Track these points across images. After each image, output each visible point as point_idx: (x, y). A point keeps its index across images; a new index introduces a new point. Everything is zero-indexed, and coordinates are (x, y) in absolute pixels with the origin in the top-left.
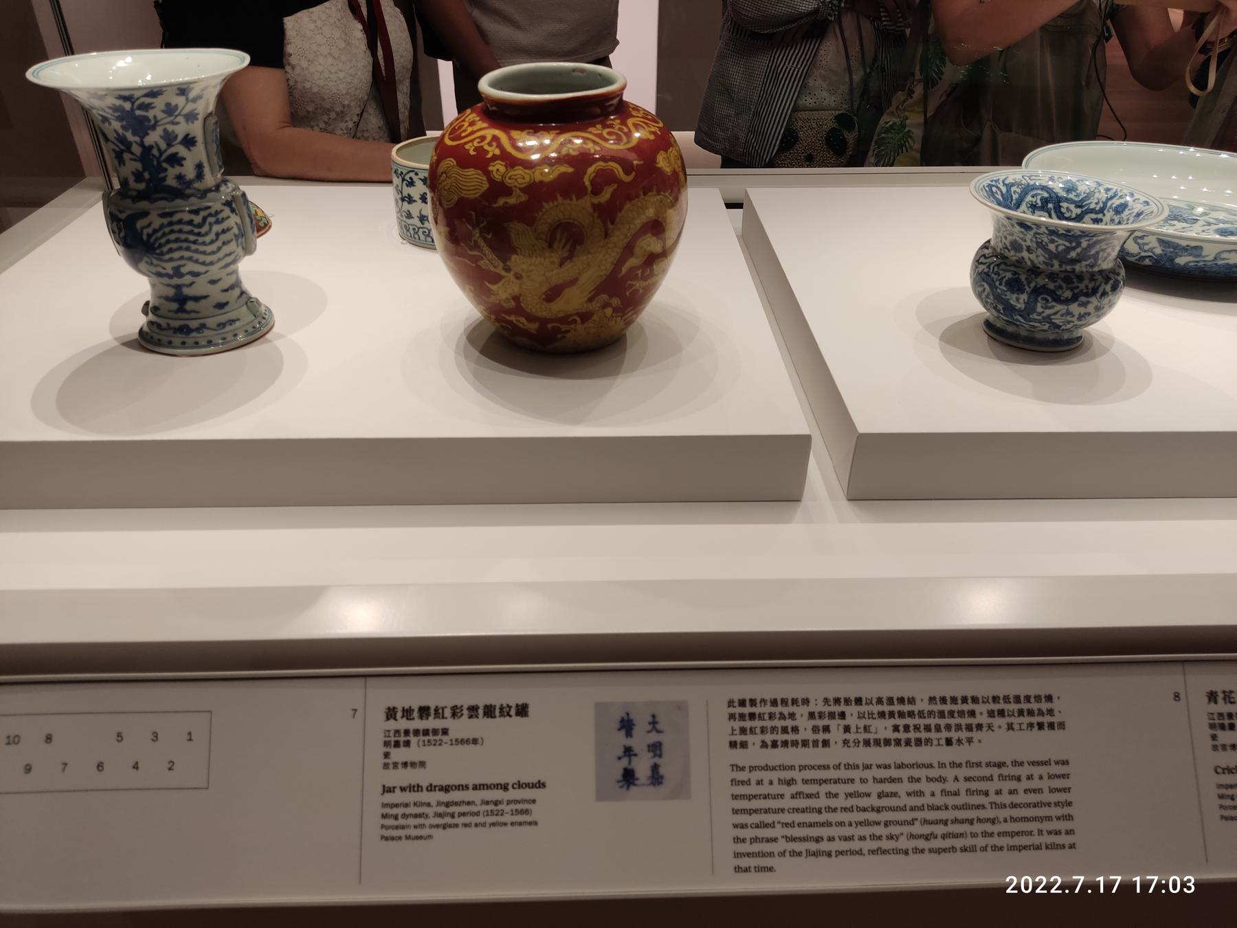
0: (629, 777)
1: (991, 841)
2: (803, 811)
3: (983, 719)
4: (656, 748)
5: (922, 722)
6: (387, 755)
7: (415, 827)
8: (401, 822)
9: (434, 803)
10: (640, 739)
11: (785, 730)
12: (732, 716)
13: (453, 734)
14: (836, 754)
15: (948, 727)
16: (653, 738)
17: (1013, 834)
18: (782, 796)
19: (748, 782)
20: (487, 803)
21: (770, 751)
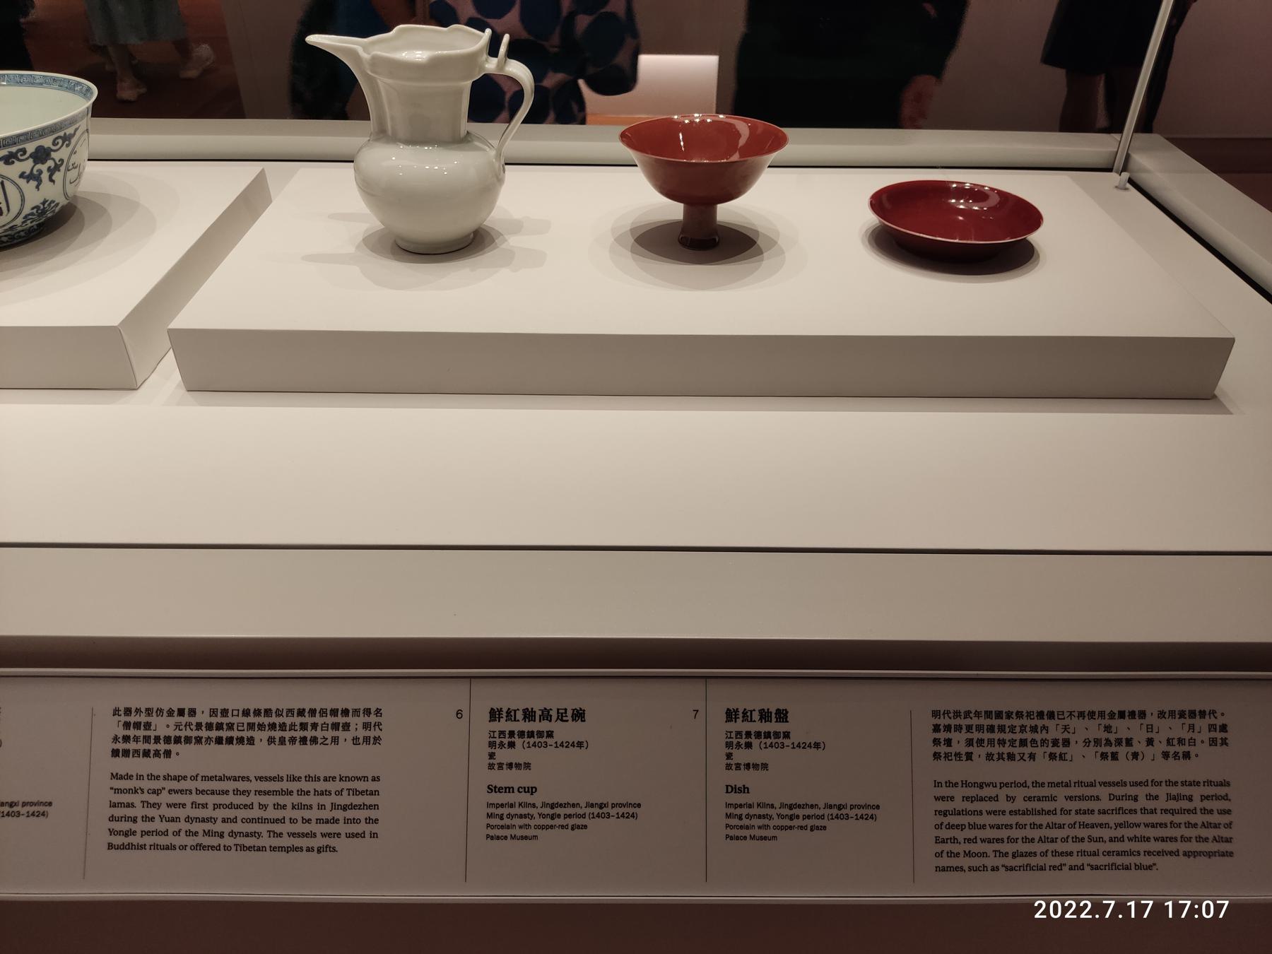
7: (521, 827)
9: (539, 804)
13: (558, 737)
15: (991, 742)
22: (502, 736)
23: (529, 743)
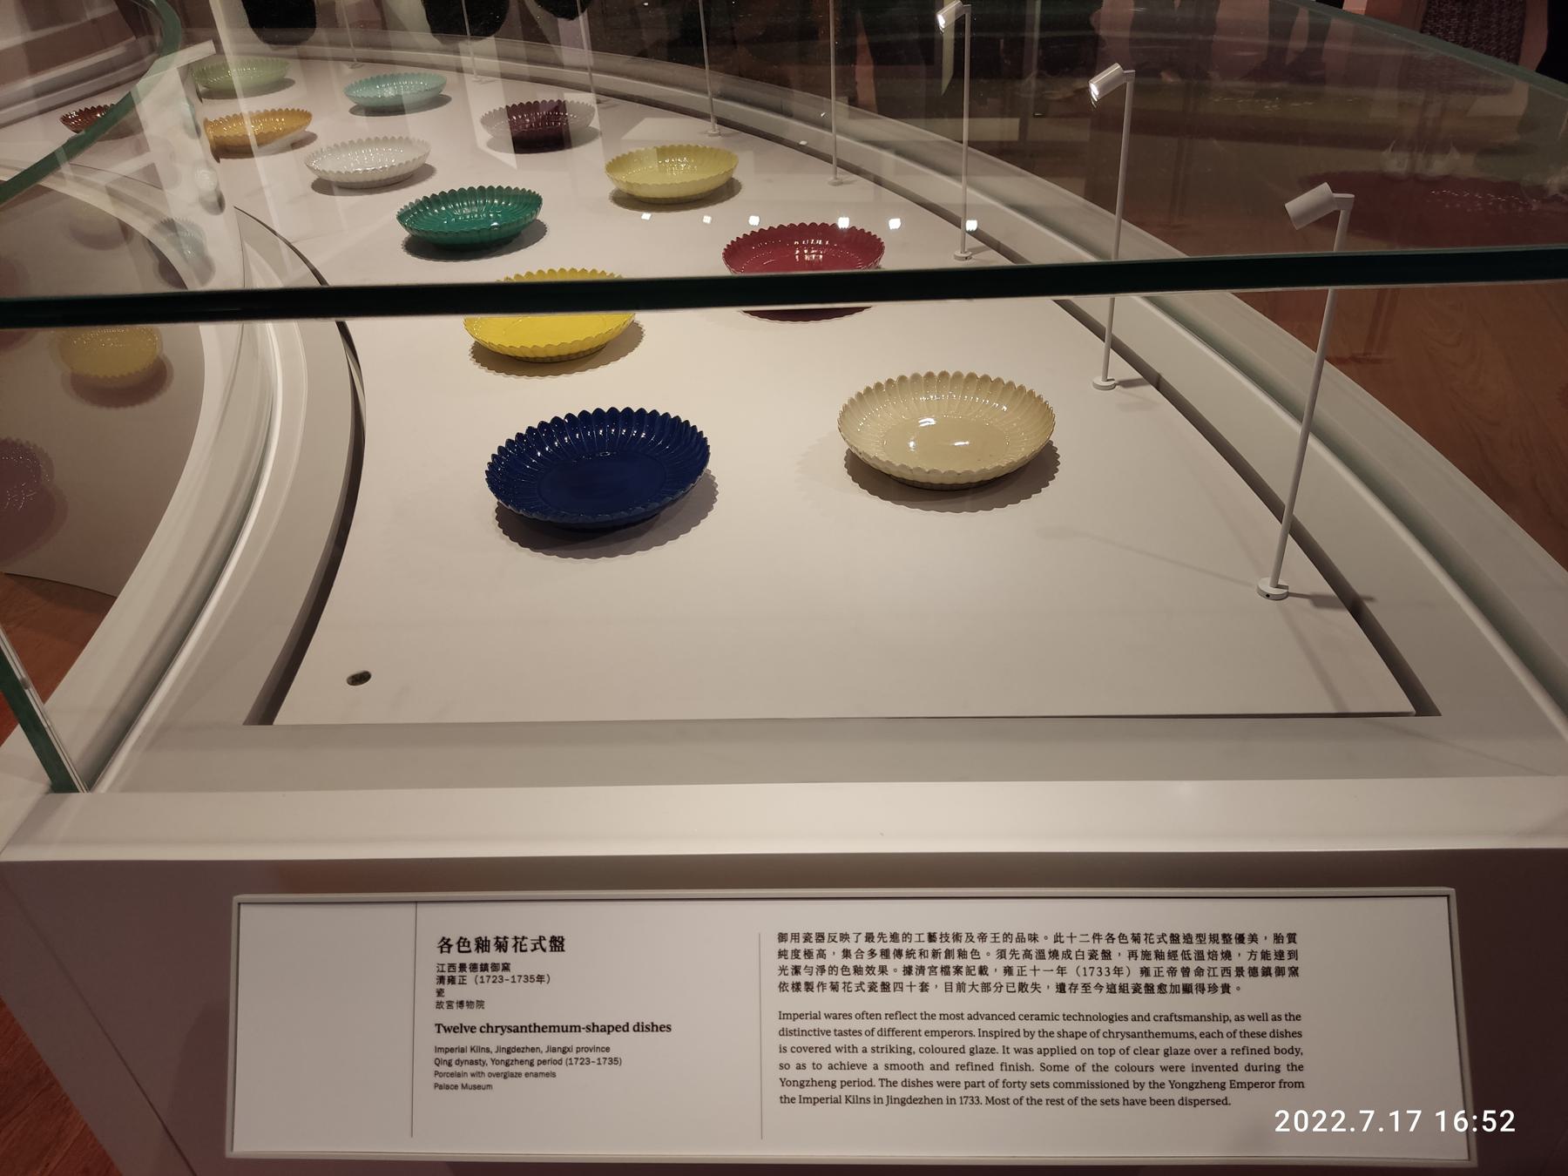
6: (440, 992)
7: (473, 1075)
8: (455, 1068)
13: (514, 970)
20: (554, 1050)
22: (452, 970)
23: (482, 977)
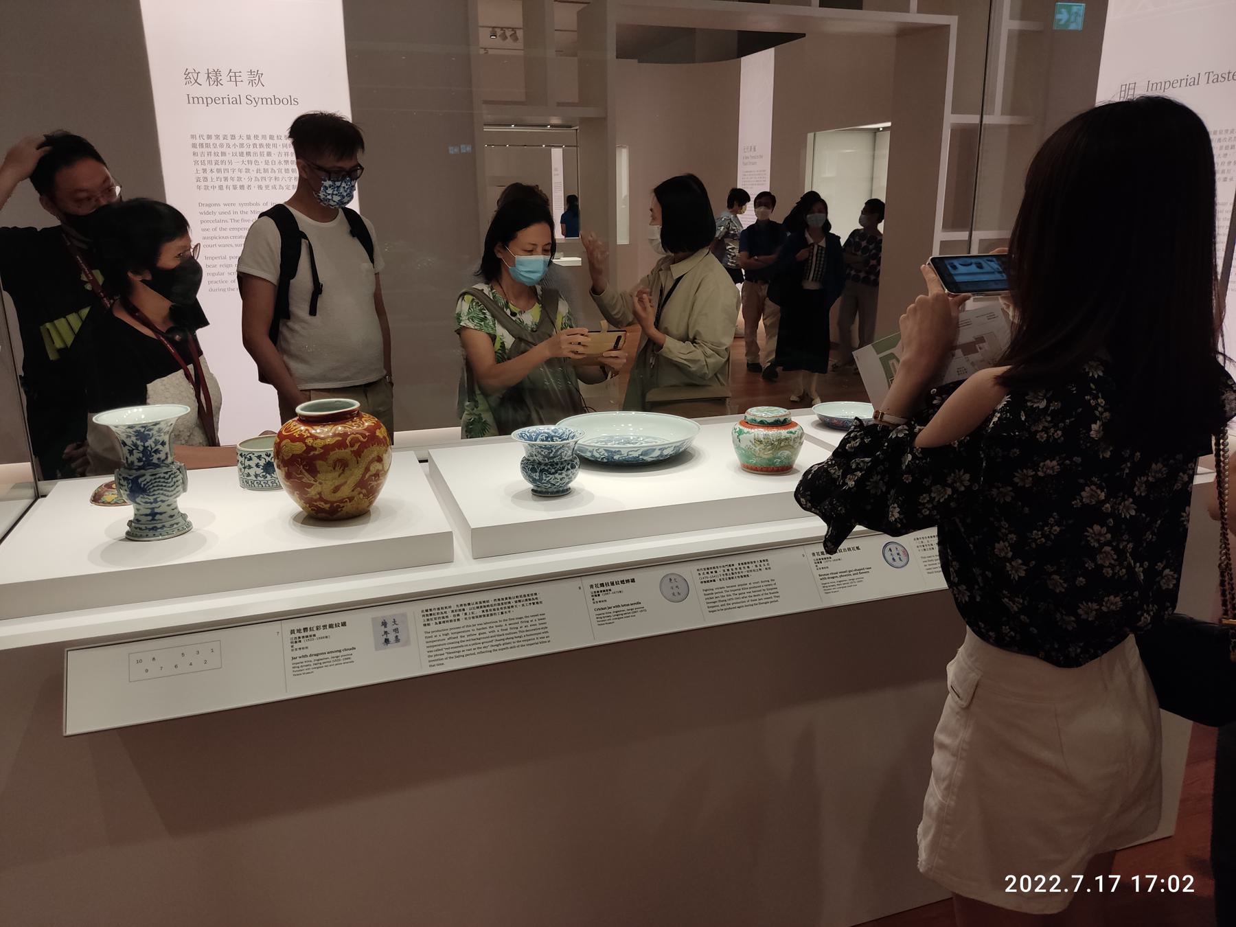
0: (387, 641)
1: (520, 644)
2: (453, 643)
3: (514, 604)
4: (396, 630)
5: (492, 608)
10: (390, 628)
11: (443, 618)
12: (423, 616)
14: (463, 623)
16: (395, 627)
17: (527, 640)
18: (444, 640)
19: (432, 637)
20: (333, 657)
21: (439, 625)
